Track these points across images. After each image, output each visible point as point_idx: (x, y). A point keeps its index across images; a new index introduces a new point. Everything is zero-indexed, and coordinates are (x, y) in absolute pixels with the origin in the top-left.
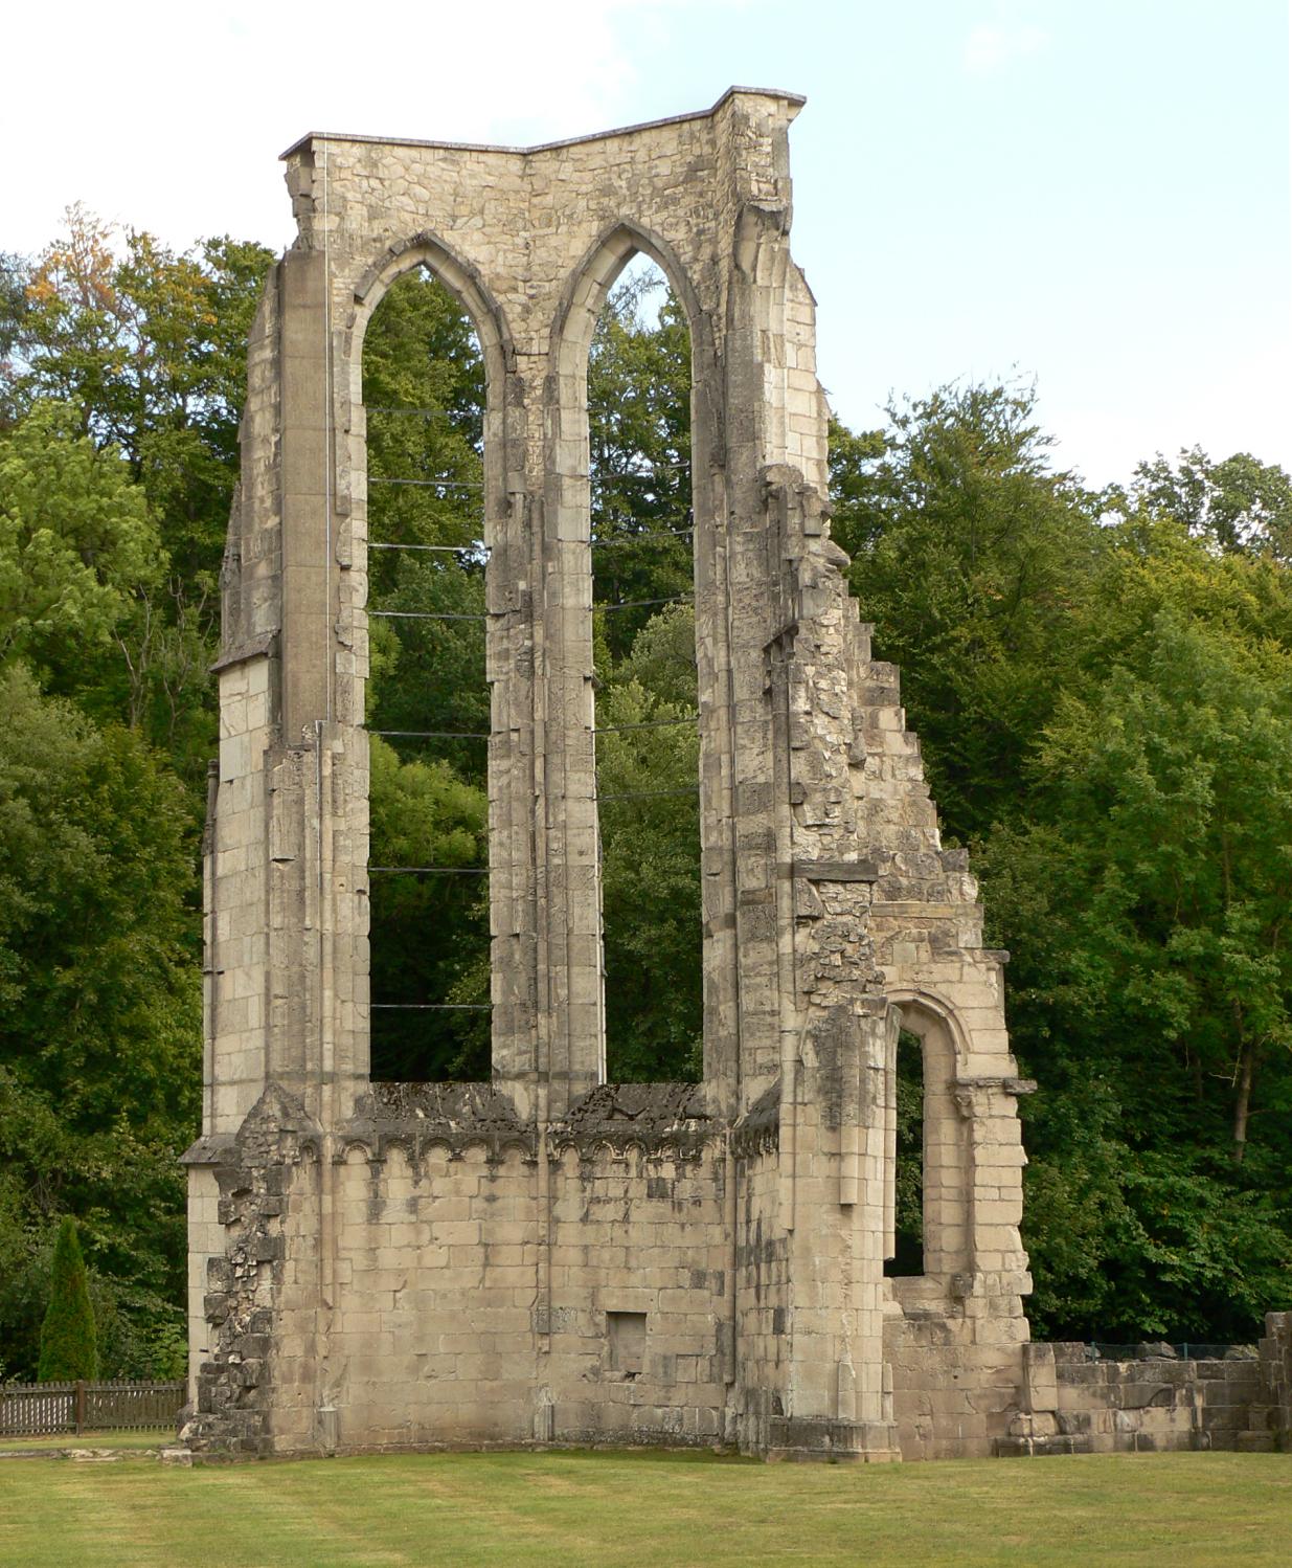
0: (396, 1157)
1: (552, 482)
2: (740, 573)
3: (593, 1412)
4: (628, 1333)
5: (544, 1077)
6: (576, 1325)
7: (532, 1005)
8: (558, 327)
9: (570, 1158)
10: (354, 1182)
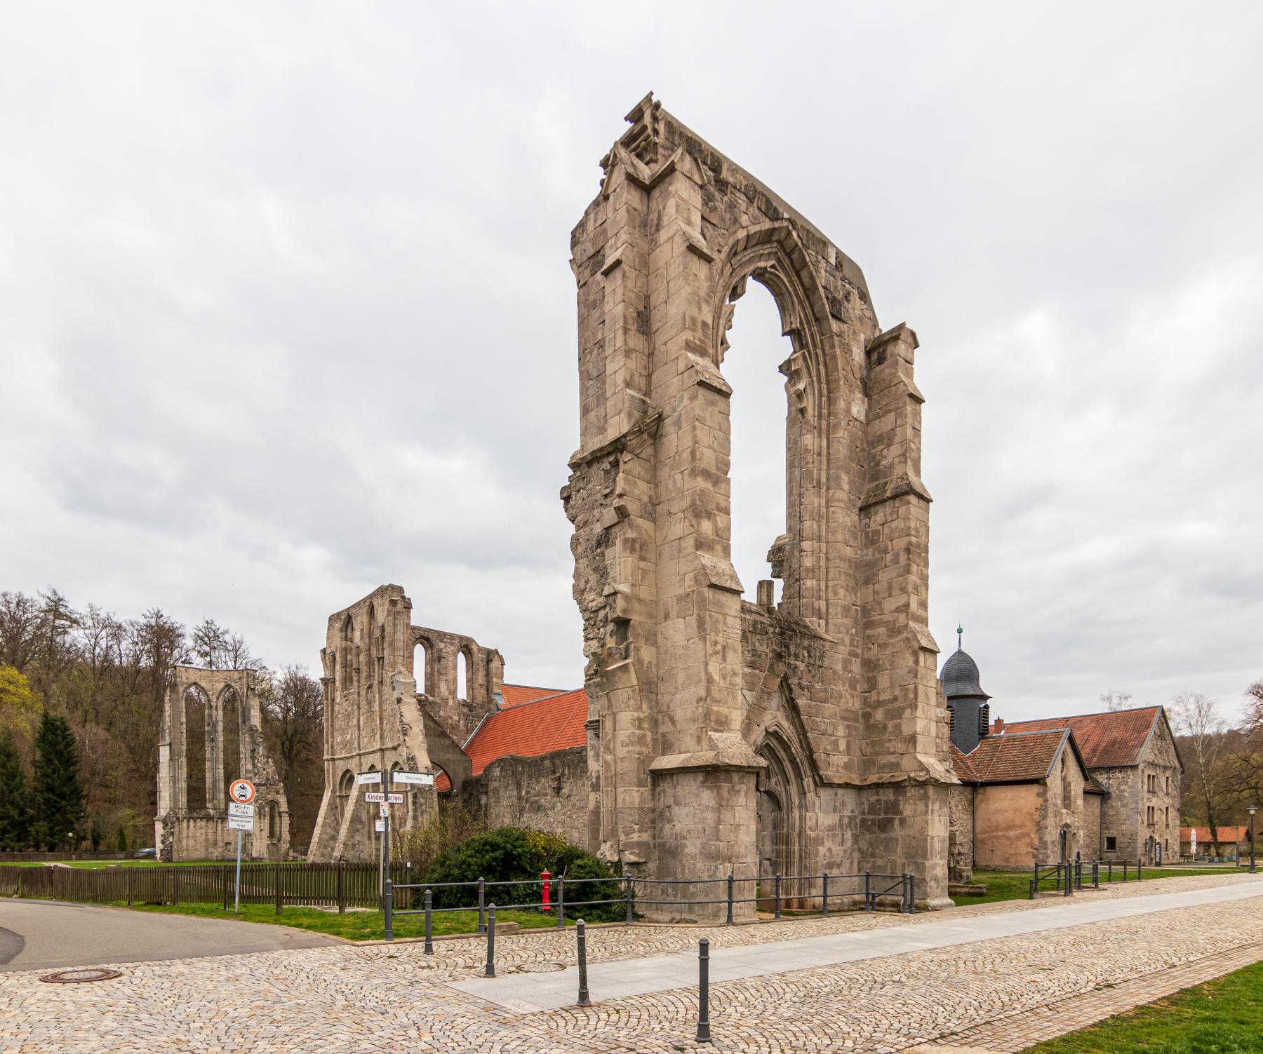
0: (192, 821)
1: (217, 721)
2: (247, 739)
3: (223, 857)
4: (229, 845)
5: (215, 809)
6: (220, 844)
7: (213, 799)
8: (218, 698)
9: (220, 821)
10: (185, 824)
